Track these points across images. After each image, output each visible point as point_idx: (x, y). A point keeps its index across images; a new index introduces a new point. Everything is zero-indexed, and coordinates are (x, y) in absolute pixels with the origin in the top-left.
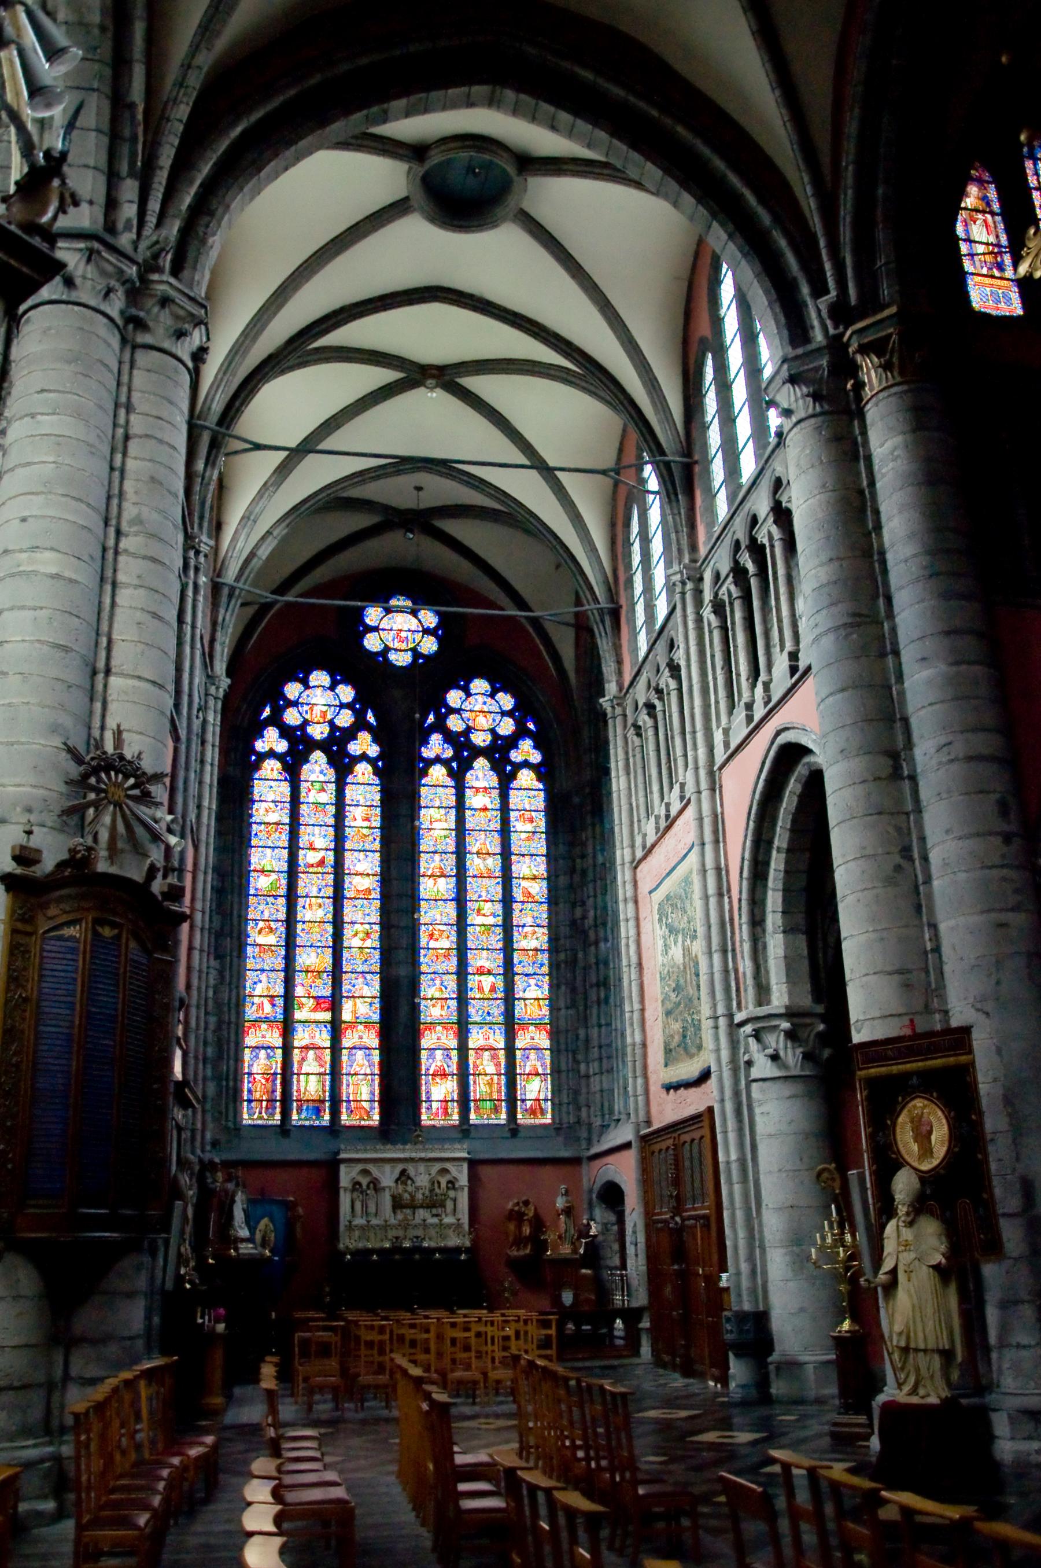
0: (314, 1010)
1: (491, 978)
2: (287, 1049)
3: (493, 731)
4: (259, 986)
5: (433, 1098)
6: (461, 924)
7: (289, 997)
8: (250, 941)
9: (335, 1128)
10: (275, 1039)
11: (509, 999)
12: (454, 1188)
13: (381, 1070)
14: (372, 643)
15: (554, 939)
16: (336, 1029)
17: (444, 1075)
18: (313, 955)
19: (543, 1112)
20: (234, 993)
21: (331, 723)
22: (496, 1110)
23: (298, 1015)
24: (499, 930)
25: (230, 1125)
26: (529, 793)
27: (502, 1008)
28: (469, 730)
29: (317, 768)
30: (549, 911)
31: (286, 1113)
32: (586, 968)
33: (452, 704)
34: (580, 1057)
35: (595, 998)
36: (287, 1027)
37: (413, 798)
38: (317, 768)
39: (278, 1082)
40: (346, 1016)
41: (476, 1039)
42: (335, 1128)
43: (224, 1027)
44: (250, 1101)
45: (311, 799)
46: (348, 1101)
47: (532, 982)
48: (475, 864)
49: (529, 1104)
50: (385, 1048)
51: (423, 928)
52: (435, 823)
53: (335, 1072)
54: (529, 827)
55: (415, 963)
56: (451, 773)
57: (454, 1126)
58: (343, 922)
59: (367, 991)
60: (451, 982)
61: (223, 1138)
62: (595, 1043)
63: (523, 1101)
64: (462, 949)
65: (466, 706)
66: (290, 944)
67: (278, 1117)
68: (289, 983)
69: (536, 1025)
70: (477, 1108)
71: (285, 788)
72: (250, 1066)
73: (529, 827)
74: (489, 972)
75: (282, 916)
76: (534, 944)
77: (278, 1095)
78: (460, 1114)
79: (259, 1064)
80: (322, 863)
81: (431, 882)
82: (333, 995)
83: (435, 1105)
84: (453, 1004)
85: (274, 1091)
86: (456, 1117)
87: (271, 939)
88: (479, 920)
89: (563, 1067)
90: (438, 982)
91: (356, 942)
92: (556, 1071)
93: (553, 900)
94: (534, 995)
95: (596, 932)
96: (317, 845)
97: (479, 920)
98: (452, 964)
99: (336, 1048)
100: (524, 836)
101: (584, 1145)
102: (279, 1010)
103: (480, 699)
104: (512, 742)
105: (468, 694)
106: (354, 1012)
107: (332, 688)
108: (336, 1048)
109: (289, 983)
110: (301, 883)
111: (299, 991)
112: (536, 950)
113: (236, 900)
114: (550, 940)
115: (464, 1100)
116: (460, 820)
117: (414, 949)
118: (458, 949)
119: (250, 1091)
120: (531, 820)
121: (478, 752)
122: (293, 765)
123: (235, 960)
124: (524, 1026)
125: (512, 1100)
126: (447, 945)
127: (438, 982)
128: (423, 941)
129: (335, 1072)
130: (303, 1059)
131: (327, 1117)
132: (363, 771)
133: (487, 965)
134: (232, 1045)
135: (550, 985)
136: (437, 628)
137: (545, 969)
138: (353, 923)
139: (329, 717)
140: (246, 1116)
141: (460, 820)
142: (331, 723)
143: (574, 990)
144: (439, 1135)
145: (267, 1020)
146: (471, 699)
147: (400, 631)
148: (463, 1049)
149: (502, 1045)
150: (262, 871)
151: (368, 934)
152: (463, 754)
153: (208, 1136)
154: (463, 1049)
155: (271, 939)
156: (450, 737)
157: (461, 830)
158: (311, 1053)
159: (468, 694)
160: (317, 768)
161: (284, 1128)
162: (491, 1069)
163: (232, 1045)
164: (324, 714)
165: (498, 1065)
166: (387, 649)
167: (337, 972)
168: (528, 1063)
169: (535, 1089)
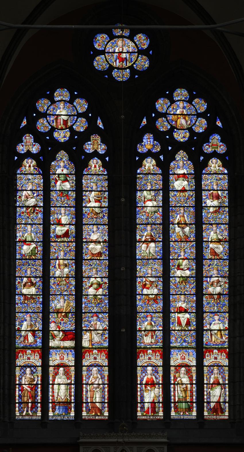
0: (63, 340)
1: (187, 316)
2: (45, 366)
3: (190, 129)
4: (25, 323)
5: (147, 400)
6: (166, 276)
11: (200, 330)
13: (109, 380)
16: (79, 352)
18: (62, 301)
19: (223, 411)
21: (71, 129)
22: (190, 409)
23: (52, 344)
24: (192, 280)
28: (173, 129)
29: (62, 164)
31: (45, 411)
36: (45, 352)
40: (85, 343)
41: (176, 359)
44: (20, 403)
46: (87, 403)
47: (216, 318)
49: (212, 405)
51: (139, 280)
52: (148, 202)
54: (216, 203)
56: (159, 164)
64: (166, 293)
65: (171, 111)
66: (46, 293)
67: (39, 414)
69: (219, 349)
70: (176, 408)
71: (39, 180)
72: (20, 379)
73: (216, 203)
74: (186, 311)
75: (40, 274)
76: (218, 289)
79: (26, 379)
80: (66, 234)
83: (146, 405)
84: (160, 334)
85: (36, 396)
86: (161, 414)
87: (33, 290)
96: (63, 221)
97: (179, 273)
99: (78, 366)
100: (212, 210)
103: (181, 104)
104: (205, 137)
105: (172, 102)
106: (91, 341)
108: (78, 366)
109: (46, 322)
110: (52, 250)
111: (52, 326)
112: (219, 294)
119: (20, 396)
120: (218, 197)
121: (178, 146)
126: (156, 291)
127: (149, 318)
130: (56, 374)
132: (95, 165)
137: (226, 308)
139: (69, 124)
140: (17, 414)
142: (71, 129)
145: (31, 347)
146: (174, 106)
147: (120, 52)
148: (166, 366)
149: (194, 363)
154: (166, 366)
155: (33, 290)
156: (158, 136)
157: (166, 207)
158: (61, 369)
159: (172, 102)
162: (185, 380)
166: (111, 68)
167: (78, 314)
169: (216, 394)
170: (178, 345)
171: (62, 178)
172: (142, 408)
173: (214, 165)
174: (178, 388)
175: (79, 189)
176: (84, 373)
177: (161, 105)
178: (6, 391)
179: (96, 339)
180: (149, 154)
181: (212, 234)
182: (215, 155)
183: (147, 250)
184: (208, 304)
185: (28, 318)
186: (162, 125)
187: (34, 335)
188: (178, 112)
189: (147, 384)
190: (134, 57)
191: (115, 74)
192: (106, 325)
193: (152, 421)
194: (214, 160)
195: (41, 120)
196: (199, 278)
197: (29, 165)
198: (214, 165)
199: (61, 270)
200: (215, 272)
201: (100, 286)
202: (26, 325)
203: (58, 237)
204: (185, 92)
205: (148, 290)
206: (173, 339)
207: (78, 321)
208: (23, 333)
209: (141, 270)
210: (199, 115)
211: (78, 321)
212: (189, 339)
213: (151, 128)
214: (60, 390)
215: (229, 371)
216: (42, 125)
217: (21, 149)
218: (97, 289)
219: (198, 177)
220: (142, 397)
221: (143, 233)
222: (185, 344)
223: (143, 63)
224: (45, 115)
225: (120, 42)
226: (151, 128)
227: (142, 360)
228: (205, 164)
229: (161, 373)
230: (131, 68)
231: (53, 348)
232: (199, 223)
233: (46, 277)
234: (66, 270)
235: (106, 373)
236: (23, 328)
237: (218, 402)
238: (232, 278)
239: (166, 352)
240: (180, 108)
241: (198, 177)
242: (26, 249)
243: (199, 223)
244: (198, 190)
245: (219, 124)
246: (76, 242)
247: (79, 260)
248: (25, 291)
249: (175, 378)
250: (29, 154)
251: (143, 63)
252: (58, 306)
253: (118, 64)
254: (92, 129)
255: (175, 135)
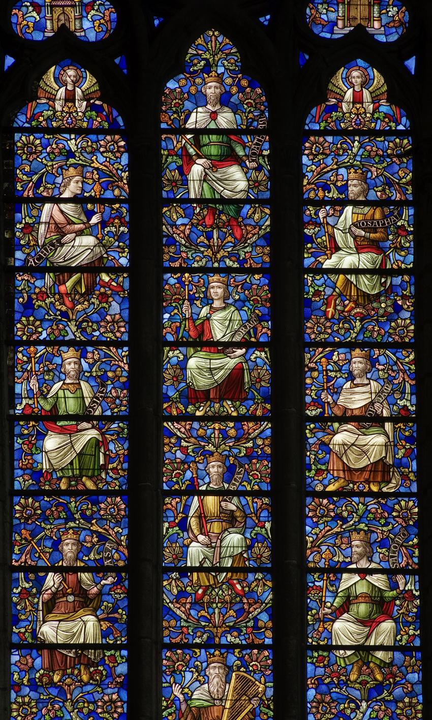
18: (215, 671)
29: (212, 89)
71: (112, 157)
75: (118, 556)
80: (232, 386)
87: (88, 627)
96: (218, 332)
132: (356, 90)
155: (88, 627)
199: (211, 540)
201: (381, 606)
203: (193, 396)
234: (234, 539)
246: (276, 418)
248: (49, 631)
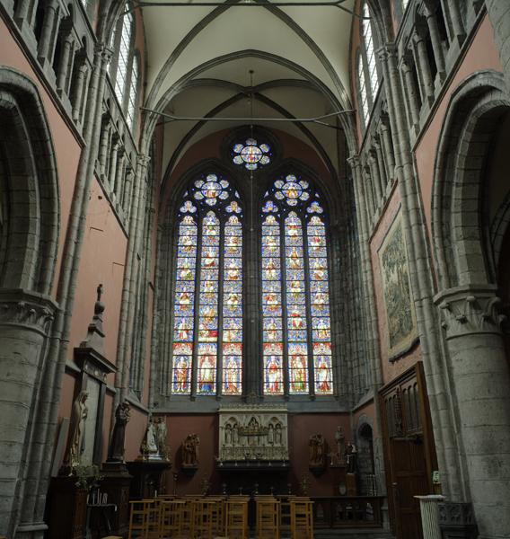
0: (208, 336)
1: (300, 319)
2: (194, 356)
3: (298, 199)
4: (181, 325)
5: (271, 380)
6: (283, 292)
7: (196, 329)
8: (176, 302)
9: (218, 397)
10: (188, 351)
11: (309, 330)
12: (280, 428)
13: (243, 366)
14: (237, 160)
15: (332, 299)
16: (220, 345)
17: (276, 369)
18: (208, 309)
19: (329, 388)
20: (168, 328)
21: (217, 198)
22: (304, 387)
23: (200, 339)
24: (303, 295)
25: (164, 394)
26: (317, 227)
27: (306, 334)
28: (286, 198)
29: (211, 219)
30: (329, 285)
31: (193, 388)
32: (349, 311)
33: (277, 187)
34: (347, 359)
35: (354, 327)
36: (195, 344)
37: (259, 233)
38: (210, 220)
39: (190, 373)
40: (225, 339)
41: (292, 350)
42: (218, 397)
43: (162, 345)
44: (175, 383)
45: (207, 234)
46: (226, 382)
47: (321, 321)
48: (291, 262)
49: (321, 384)
50: (245, 356)
51: (264, 295)
52: (270, 243)
53: (219, 367)
54: (317, 244)
55: (261, 312)
56: (277, 219)
57: (281, 396)
58: (223, 293)
59: (235, 327)
60: (279, 321)
61: (160, 402)
62: (355, 350)
63: (318, 382)
64: (283, 305)
65: (284, 187)
66: (196, 303)
67: (189, 391)
68: (196, 324)
69: (324, 343)
70: (293, 386)
71: (195, 229)
72: (176, 365)
73: (317, 244)
74: (299, 316)
75: (193, 290)
76: (322, 301)
77: (189, 379)
78: (284, 389)
79: (180, 364)
80: (213, 264)
81: (267, 272)
82: (218, 329)
83: (271, 384)
84: (280, 333)
85: (187, 377)
86: (282, 391)
87: (187, 302)
88: (293, 290)
89: (339, 364)
90: (272, 321)
91: (230, 302)
92: (335, 366)
93: (331, 279)
94: (322, 327)
95: (354, 293)
96: (210, 255)
97: (293, 290)
98: (280, 313)
99: (219, 355)
100: (315, 248)
101: (351, 405)
102: (191, 337)
103: (291, 184)
104: (308, 203)
105: (285, 182)
106: (229, 337)
107: (218, 182)
108: (219, 355)
109: (196, 324)
110: (202, 274)
111: (201, 327)
112: (323, 304)
113: (169, 282)
114: (330, 300)
115: (286, 382)
116: (282, 241)
117: (259, 305)
118: (282, 305)
119: (175, 377)
120: (319, 241)
121: (291, 208)
122: (198, 219)
123: (168, 312)
124: (318, 343)
125: (311, 381)
126: (276, 303)
127: (272, 321)
128: (264, 302)
129: (219, 367)
130: (203, 361)
131: (215, 391)
132: (233, 220)
133: (297, 312)
134: (166, 355)
135: (331, 323)
136: (269, 152)
137: (327, 314)
138: (228, 293)
139: (216, 195)
140: (173, 390)
141: (282, 241)
142: (217, 198)
143: (343, 324)
144: (274, 400)
145: (184, 342)
146: (287, 185)
147: (251, 155)
148: (285, 355)
149: (306, 353)
150: (183, 269)
151: (236, 298)
152: (283, 210)
153: (152, 400)
154: (285, 355)
155: (187, 302)
156: (276, 202)
157: (282, 246)
158: (207, 358)
159: (285, 182)
160: (210, 220)
161: (192, 397)
162: (300, 366)
163: (166, 355)
164: (214, 194)
165: (304, 364)
166: (245, 163)
167: (220, 317)
168: (318, 363)
169: (324, 376)
170: (294, 340)
171: (211, 228)
172: (268, 386)
173: (315, 220)
174: (295, 371)
175: (222, 235)
176: (224, 361)
177: (278, 184)
178: (165, 374)
179: (233, 336)
180: (271, 213)
181: (315, 264)
182: (315, 214)
183: (270, 274)
184: (315, 312)
185: (184, 321)
186: (279, 196)
187: (188, 334)
188: (290, 188)
189: (271, 369)
190: (260, 157)
191: (247, 166)
192: (240, 326)
193: (275, 396)
194: (315, 218)
195: (197, 193)
196: (307, 294)
197: (188, 220)
198: (315, 220)
199: (208, 288)
200: (319, 289)
201: (236, 298)
202: (182, 326)
203: (206, 265)
204: (294, 178)
205: (271, 301)
206: (290, 336)
207: (220, 323)
208: (179, 332)
209: (265, 287)
210: (303, 190)
211: (220, 323)
212: (302, 336)
213: (272, 198)
214: (206, 373)
215: (333, 358)
216: (198, 196)
217: (183, 210)
218: (233, 301)
219: (304, 227)
220: (267, 378)
221: (267, 263)
222: (299, 340)
223: (266, 160)
224: (200, 190)
225: (250, 148)
226: (272, 198)
227: (267, 351)
228: (309, 220)
229: (281, 361)
230: (258, 163)
231: (201, 342)
232: (306, 257)
233: (197, 293)
234: (212, 288)
235: (240, 361)
236: (180, 328)
237: (325, 382)
238: (331, 293)
239: (285, 344)
240: (291, 186)
241: (304, 227)
242: (184, 274)
243: (306, 257)
244: (305, 236)
245: (317, 195)
246: (219, 269)
247: (221, 281)
248: (181, 302)
249: (292, 364)
250: (188, 213)
251: (266, 160)
252: (206, 313)
253: (249, 161)
254: (231, 198)
255: (288, 202)
